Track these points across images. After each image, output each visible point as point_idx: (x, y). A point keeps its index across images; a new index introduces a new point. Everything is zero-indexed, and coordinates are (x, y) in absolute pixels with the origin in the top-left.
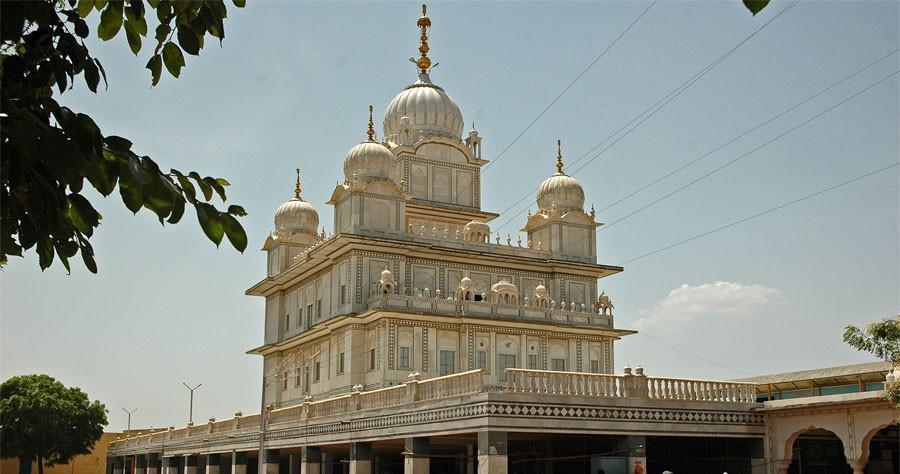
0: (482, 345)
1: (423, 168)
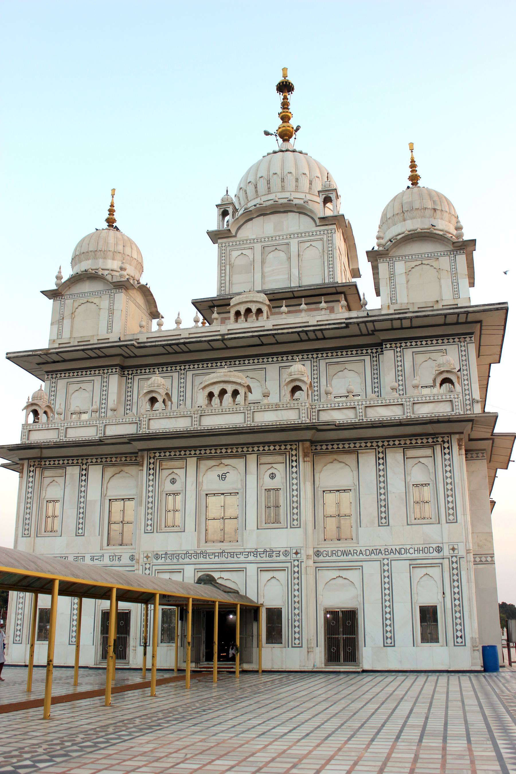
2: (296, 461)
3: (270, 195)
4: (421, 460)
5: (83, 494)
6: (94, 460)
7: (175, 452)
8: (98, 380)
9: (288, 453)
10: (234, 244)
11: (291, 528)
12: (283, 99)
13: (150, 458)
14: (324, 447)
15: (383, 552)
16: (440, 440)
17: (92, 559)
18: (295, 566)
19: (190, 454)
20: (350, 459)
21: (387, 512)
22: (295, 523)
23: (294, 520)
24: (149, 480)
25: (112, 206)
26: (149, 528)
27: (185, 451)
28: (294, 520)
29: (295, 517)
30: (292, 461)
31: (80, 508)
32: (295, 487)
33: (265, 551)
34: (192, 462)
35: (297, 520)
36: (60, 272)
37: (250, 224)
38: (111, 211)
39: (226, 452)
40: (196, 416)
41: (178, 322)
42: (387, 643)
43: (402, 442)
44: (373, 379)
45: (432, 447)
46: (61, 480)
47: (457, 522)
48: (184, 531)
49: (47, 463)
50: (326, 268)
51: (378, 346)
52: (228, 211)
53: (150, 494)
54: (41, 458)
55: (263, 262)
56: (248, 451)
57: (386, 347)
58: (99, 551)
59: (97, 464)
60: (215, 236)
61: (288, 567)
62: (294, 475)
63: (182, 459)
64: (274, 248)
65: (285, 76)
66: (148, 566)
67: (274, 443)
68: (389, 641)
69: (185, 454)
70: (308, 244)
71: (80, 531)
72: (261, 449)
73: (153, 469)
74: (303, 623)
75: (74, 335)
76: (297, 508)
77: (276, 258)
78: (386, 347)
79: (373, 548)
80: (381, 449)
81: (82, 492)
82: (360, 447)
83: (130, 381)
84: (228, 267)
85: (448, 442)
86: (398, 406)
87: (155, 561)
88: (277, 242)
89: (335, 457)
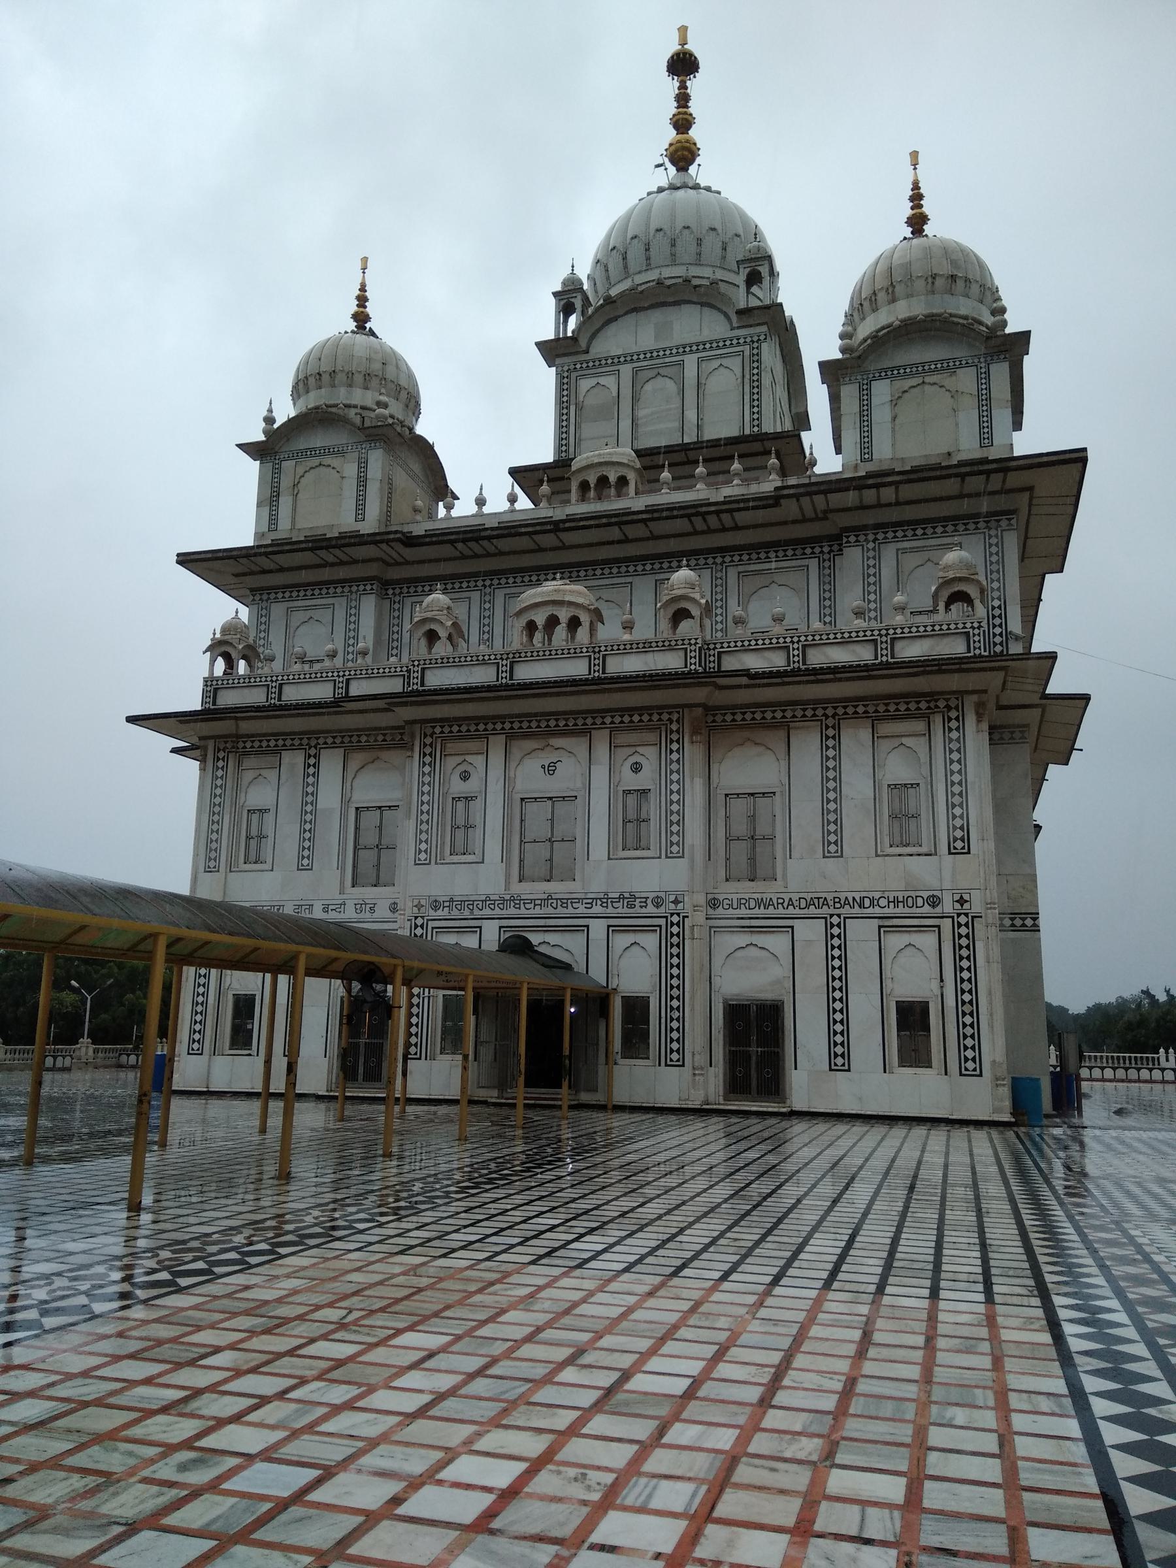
0: (465, 776)
1: (609, 381)
2: (678, 741)
3: (649, 272)
4: (904, 740)
5: (310, 799)
6: (330, 740)
7: (468, 725)
8: (340, 604)
9: (663, 728)
10: (584, 365)
11: (667, 857)
12: (679, 88)
13: (425, 736)
14: (729, 718)
15: (831, 903)
16: (942, 704)
17: (326, 909)
18: (672, 924)
19: (494, 729)
20: (776, 738)
21: (839, 832)
22: (675, 848)
23: (672, 844)
24: (424, 774)
25: (363, 289)
26: (423, 856)
27: (486, 724)
28: (672, 844)
29: (675, 839)
30: (672, 741)
31: (306, 822)
32: (675, 787)
33: (622, 897)
34: (497, 744)
35: (678, 844)
36: (270, 411)
37: (613, 328)
38: (362, 300)
39: (557, 726)
40: (504, 662)
41: (480, 502)
42: (836, 1065)
43: (871, 709)
44: (822, 599)
45: (927, 717)
46: (272, 775)
47: (969, 853)
48: (483, 862)
49: (248, 745)
50: (747, 407)
51: (836, 542)
52: (573, 304)
53: (425, 798)
54: (238, 736)
55: (635, 399)
56: (594, 724)
57: (848, 542)
58: (337, 896)
59: (334, 746)
60: (551, 351)
61: (660, 926)
62: (675, 766)
63: (479, 737)
64: (656, 371)
65: (683, 42)
66: (419, 921)
67: (640, 710)
68: (839, 1061)
69: (486, 730)
70: (718, 362)
71: (305, 862)
72: (617, 719)
73: (430, 755)
74: (686, 1024)
75: (298, 526)
76: (678, 823)
77: (659, 393)
78: (848, 542)
79: (811, 895)
80: (830, 722)
81: (309, 797)
82: (794, 716)
83: (396, 606)
84: (573, 408)
85: (957, 708)
86: (865, 644)
87: (432, 912)
88: (661, 361)
89: (746, 734)
